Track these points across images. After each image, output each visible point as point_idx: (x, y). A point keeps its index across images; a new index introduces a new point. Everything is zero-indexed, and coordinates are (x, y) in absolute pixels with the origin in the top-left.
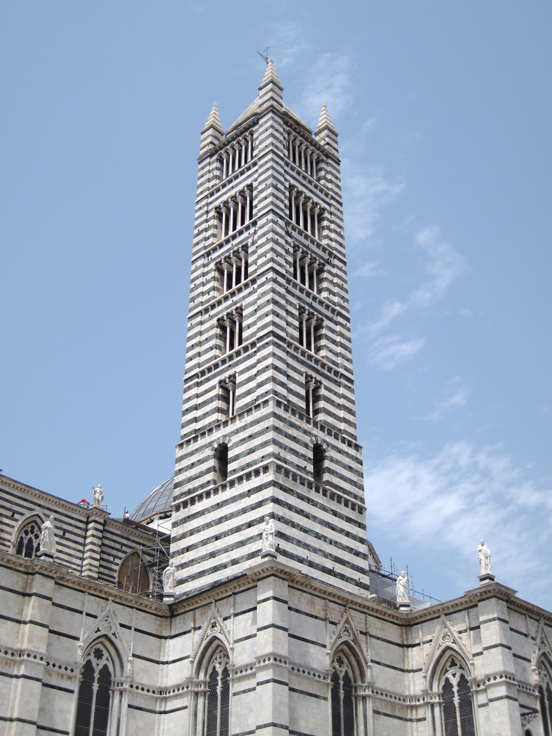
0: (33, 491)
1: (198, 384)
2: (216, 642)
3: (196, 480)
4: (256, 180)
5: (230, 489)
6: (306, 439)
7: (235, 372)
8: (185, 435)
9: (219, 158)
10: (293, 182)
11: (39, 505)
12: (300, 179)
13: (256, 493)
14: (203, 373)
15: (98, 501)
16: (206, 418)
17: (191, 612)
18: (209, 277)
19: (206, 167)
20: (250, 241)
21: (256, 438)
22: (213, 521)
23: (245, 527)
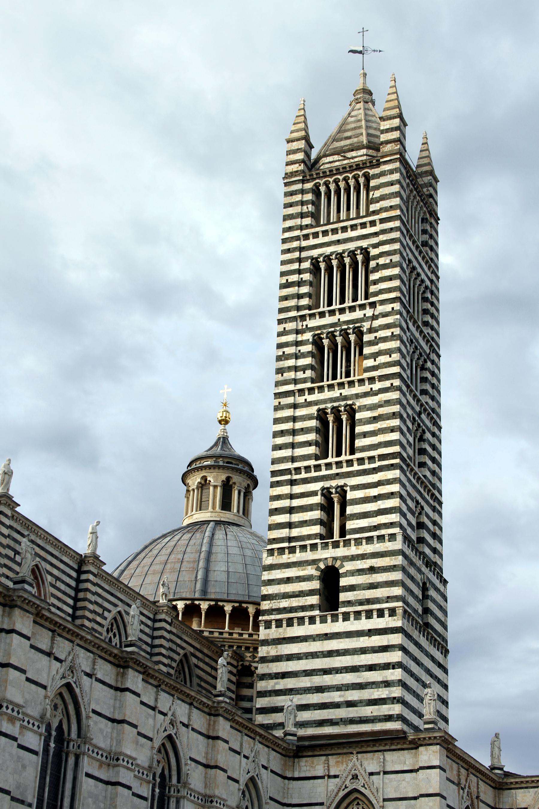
0: (119, 585)
1: (292, 483)
2: (356, 795)
3: (294, 599)
4: (375, 246)
5: (343, 621)
6: (418, 577)
7: (345, 485)
8: (274, 539)
9: (314, 188)
10: (411, 256)
11: (121, 600)
12: (413, 248)
13: (379, 635)
14: (298, 470)
15: (166, 596)
16: (303, 527)
17: (324, 758)
19: (296, 194)
20: (366, 325)
21: (378, 573)
22: (319, 652)
23: (364, 669)
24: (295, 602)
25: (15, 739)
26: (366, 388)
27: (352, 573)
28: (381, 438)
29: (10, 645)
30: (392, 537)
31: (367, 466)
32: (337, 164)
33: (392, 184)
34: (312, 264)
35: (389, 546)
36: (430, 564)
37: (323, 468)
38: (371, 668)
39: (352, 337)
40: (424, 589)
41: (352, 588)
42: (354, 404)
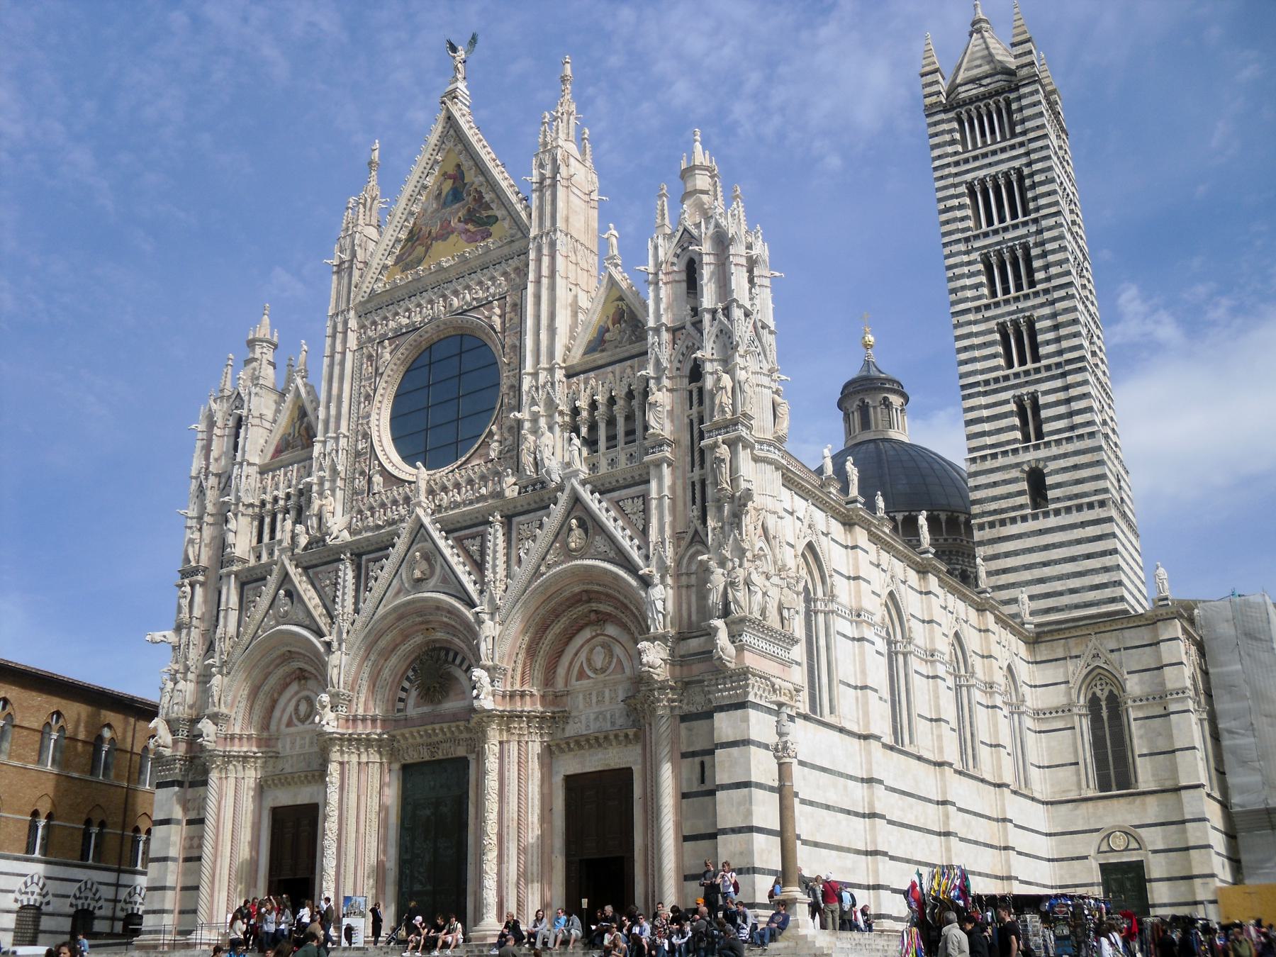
1: (985, 394)
4: (1029, 164)
6: (1114, 470)
7: (1036, 391)
14: (987, 382)
18: (973, 268)
20: (1031, 240)
24: (1004, 504)
25: (873, 643)
26: (1042, 299)
27: (1057, 472)
28: (1065, 344)
29: (856, 559)
30: (1092, 435)
31: (1054, 372)
32: (974, 92)
33: (1034, 104)
34: (967, 188)
35: (1088, 443)
36: (1117, 457)
37: (1012, 377)
38: (1088, 556)
39: (1019, 253)
40: (1119, 481)
41: (1058, 485)
42: (1032, 315)
